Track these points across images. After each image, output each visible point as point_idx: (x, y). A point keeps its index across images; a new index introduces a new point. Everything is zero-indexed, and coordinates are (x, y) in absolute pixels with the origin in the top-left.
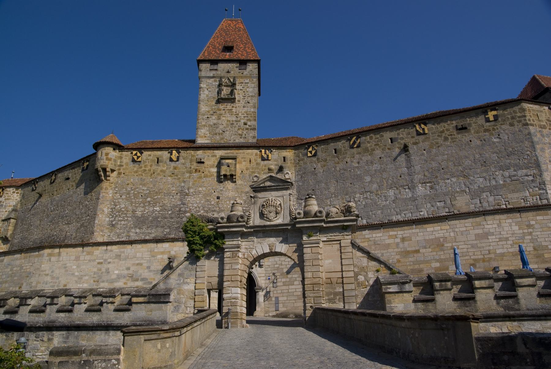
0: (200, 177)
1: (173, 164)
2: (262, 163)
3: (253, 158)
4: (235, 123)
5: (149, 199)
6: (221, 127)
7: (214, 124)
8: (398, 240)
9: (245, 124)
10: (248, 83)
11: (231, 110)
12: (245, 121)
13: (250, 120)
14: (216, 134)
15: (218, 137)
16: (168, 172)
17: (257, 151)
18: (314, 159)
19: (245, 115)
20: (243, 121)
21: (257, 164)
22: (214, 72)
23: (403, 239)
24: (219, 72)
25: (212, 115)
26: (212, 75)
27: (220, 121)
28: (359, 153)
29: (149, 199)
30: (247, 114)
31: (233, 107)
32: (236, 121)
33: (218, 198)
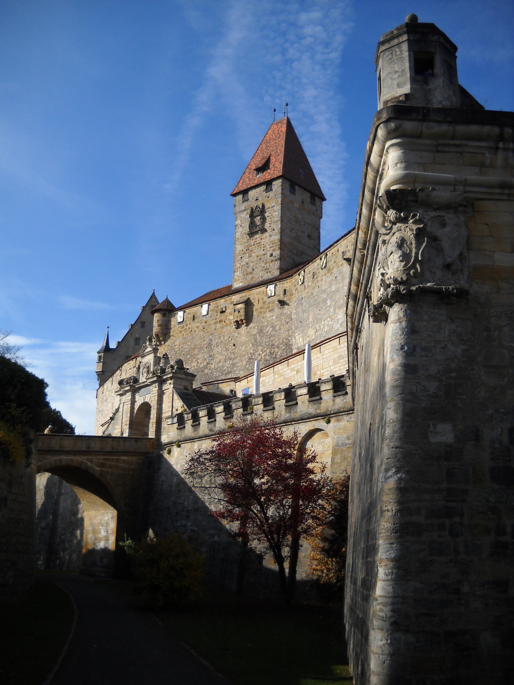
0: (223, 328)
1: (204, 319)
2: (268, 300)
3: (260, 296)
4: (262, 257)
5: (188, 357)
6: (251, 265)
7: (247, 263)
8: (295, 373)
9: (271, 255)
10: (274, 206)
11: (260, 243)
12: (271, 252)
13: (274, 250)
14: (247, 274)
15: (250, 276)
16: (201, 328)
17: (263, 289)
18: (303, 287)
19: (271, 246)
20: (269, 254)
21: (264, 303)
22: (245, 204)
23: (298, 372)
24: (248, 203)
25: (245, 253)
26: (243, 208)
27: (251, 259)
28: (325, 275)
29: (188, 357)
30: (273, 244)
31: (261, 239)
32: (264, 255)
33: (234, 345)
